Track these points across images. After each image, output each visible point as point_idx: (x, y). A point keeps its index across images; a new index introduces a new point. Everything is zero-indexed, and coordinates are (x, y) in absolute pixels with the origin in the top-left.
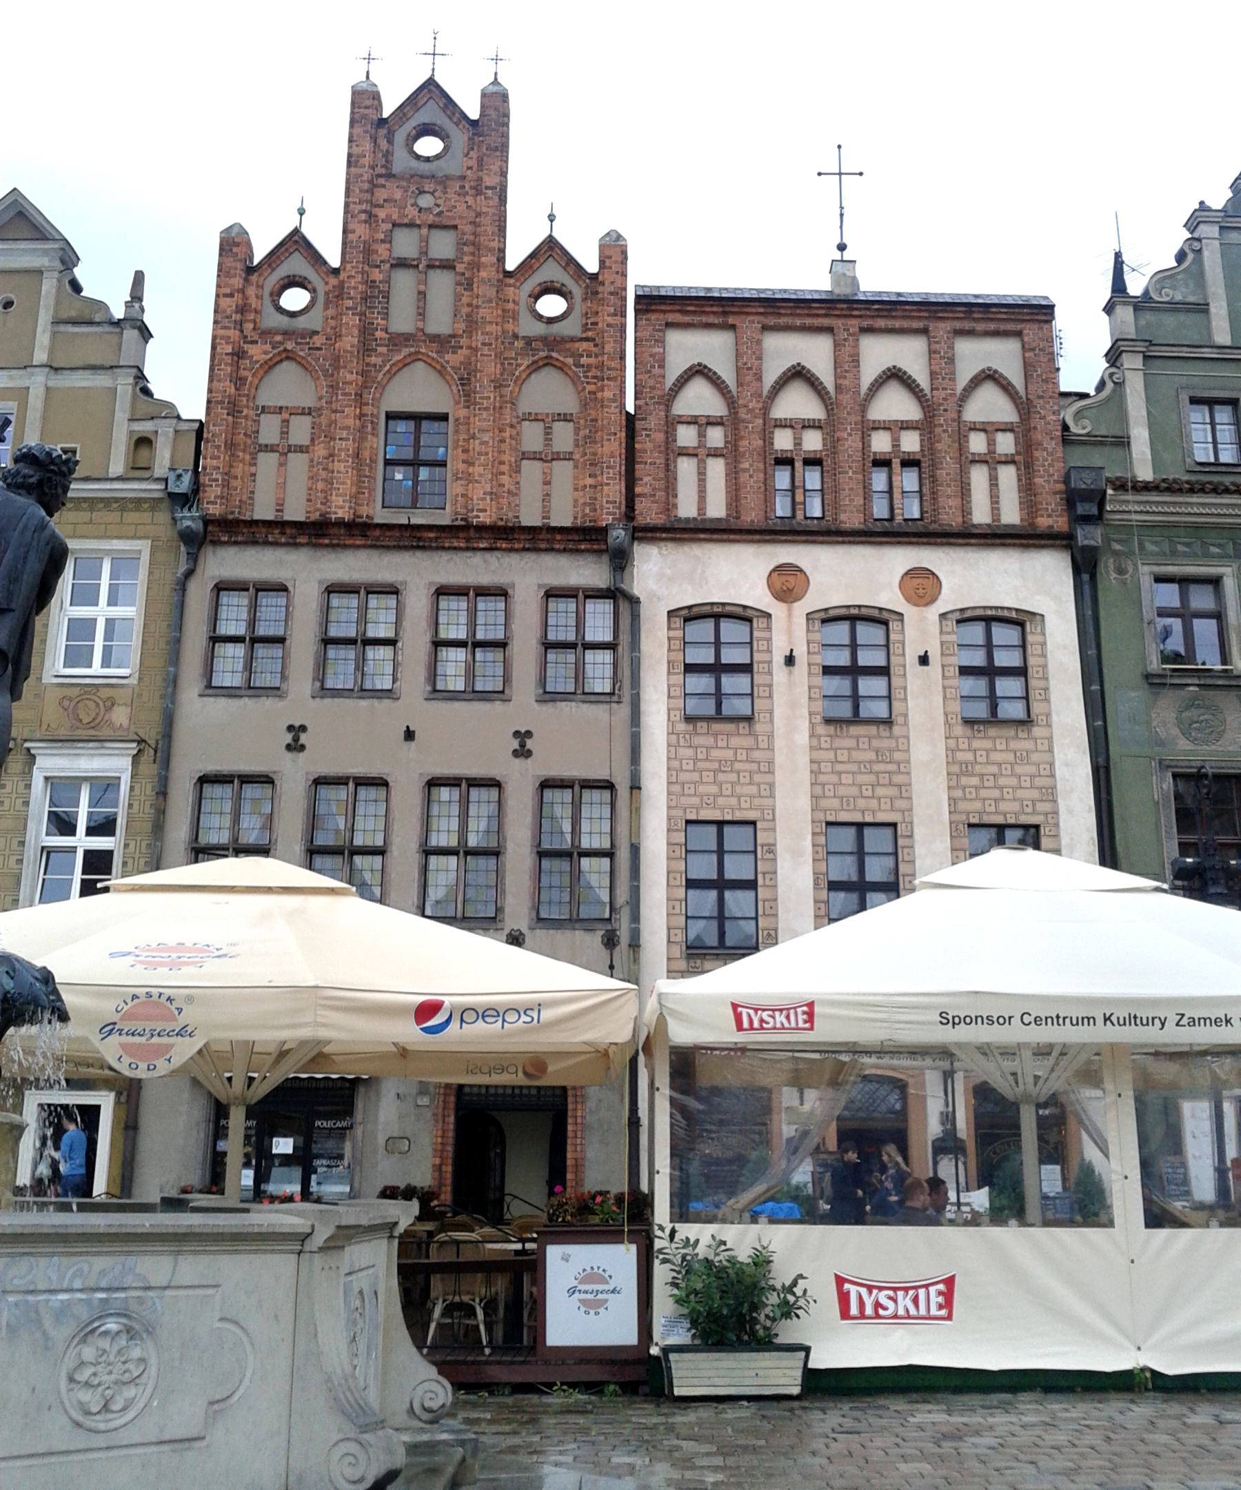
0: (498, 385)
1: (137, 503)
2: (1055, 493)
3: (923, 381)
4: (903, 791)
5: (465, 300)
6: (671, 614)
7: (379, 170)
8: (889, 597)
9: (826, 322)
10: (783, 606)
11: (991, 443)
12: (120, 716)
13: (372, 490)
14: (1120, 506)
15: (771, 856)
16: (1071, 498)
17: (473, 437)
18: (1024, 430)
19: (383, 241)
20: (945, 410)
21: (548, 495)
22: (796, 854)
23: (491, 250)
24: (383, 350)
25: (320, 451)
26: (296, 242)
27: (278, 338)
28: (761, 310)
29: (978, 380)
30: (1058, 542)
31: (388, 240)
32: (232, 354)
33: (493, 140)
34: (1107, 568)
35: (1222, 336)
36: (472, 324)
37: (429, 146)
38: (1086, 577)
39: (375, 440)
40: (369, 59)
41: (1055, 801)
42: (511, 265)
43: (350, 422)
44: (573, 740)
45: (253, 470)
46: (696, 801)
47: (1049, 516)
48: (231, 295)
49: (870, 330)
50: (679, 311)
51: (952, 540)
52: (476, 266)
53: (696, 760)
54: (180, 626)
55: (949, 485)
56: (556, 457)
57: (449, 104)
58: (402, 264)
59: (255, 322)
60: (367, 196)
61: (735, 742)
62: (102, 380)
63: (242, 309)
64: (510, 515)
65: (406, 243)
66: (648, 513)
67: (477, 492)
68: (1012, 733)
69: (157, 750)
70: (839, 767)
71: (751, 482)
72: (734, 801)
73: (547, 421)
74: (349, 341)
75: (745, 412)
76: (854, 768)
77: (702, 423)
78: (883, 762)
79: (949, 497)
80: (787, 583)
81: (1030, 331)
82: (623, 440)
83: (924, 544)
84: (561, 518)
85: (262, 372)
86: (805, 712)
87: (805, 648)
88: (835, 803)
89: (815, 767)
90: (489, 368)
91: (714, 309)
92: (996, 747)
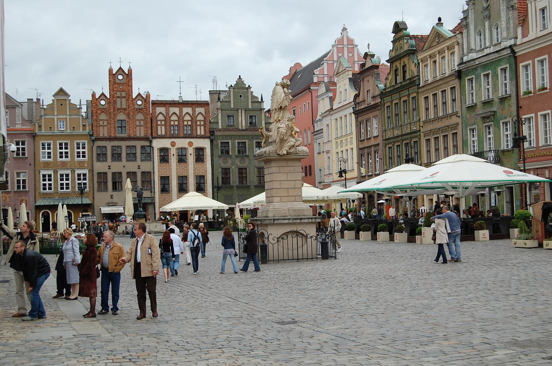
0: (133, 116)
1: (84, 135)
8: (187, 146)
12: (86, 165)
14: (217, 133)
16: (210, 132)
18: (204, 121)
29: (198, 114)
34: (215, 142)
35: (232, 107)
42: (134, 98)
44: (146, 166)
54: (92, 153)
57: (123, 71)
58: (118, 97)
62: (78, 117)
65: (118, 94)
66: (154, 135)
67: (131, 132)
69: (91, 171)
71: (168, 130)
73: (140, 120)
74: (112, 110)
75: (167, 119)
77: (161, 121)
80: (173, 144)
81: (206, 107)
84: (142, 135)
90: (132, 114)
92: (200, 165)
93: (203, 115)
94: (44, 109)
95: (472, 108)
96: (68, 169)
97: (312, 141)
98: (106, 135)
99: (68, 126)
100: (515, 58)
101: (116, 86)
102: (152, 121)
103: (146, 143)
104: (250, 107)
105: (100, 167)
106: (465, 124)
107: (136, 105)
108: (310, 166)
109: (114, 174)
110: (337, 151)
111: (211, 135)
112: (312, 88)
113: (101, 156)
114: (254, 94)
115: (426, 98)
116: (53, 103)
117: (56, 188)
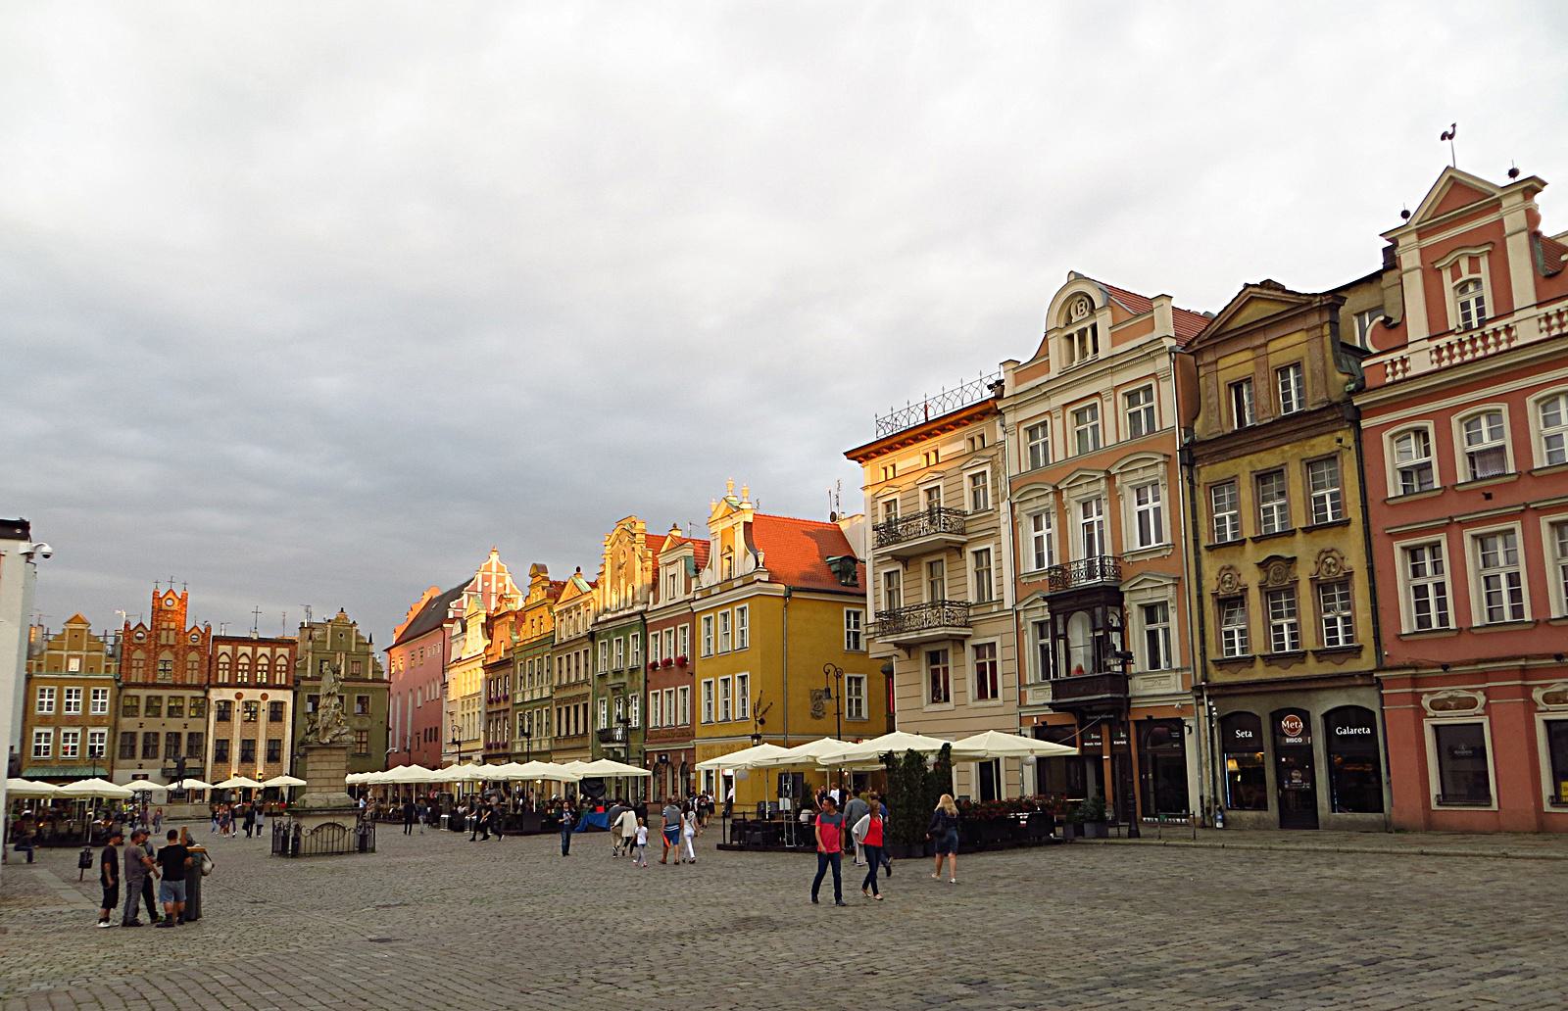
4: (257, 734)
14: (303, 683)
16: (294, 681)
18: (287, 666)
26: (141, 624)
29: (279, 657)
34: (299, 695)
35: (328, 648)
36: (178, 643)
37: (169, 602)
44: (196, 726)
57: (174, 594)
58: (164, 629)
65: (165, 625)
66: (212, 682)
69: (114, 729)
74: (152, 647)
75: (234, 661)
77: (224, 664)
80: (239, 696)
84: (195, 682)
92: (276, 725)
93: (285, 657)
94: (49, 641)
95: (603, 677)
96: (79, 726)
97: (441, 696)
98: (140, 681)
99: (84, 667)
100: (646, 625)
101: (162, 614)
102: (212, 661)
103: (199, 694)
104: (353, 650)
105: (127, 724)
106: (596, 695)
108: (436, 728)
109: (147, 734)
110: (463, 713)
111: (294, 685)
112: (445, 625)
113: (131, 711)
114: (361, 633)
115: (560, 659)
116: (63, 634)
117: (56, 751)
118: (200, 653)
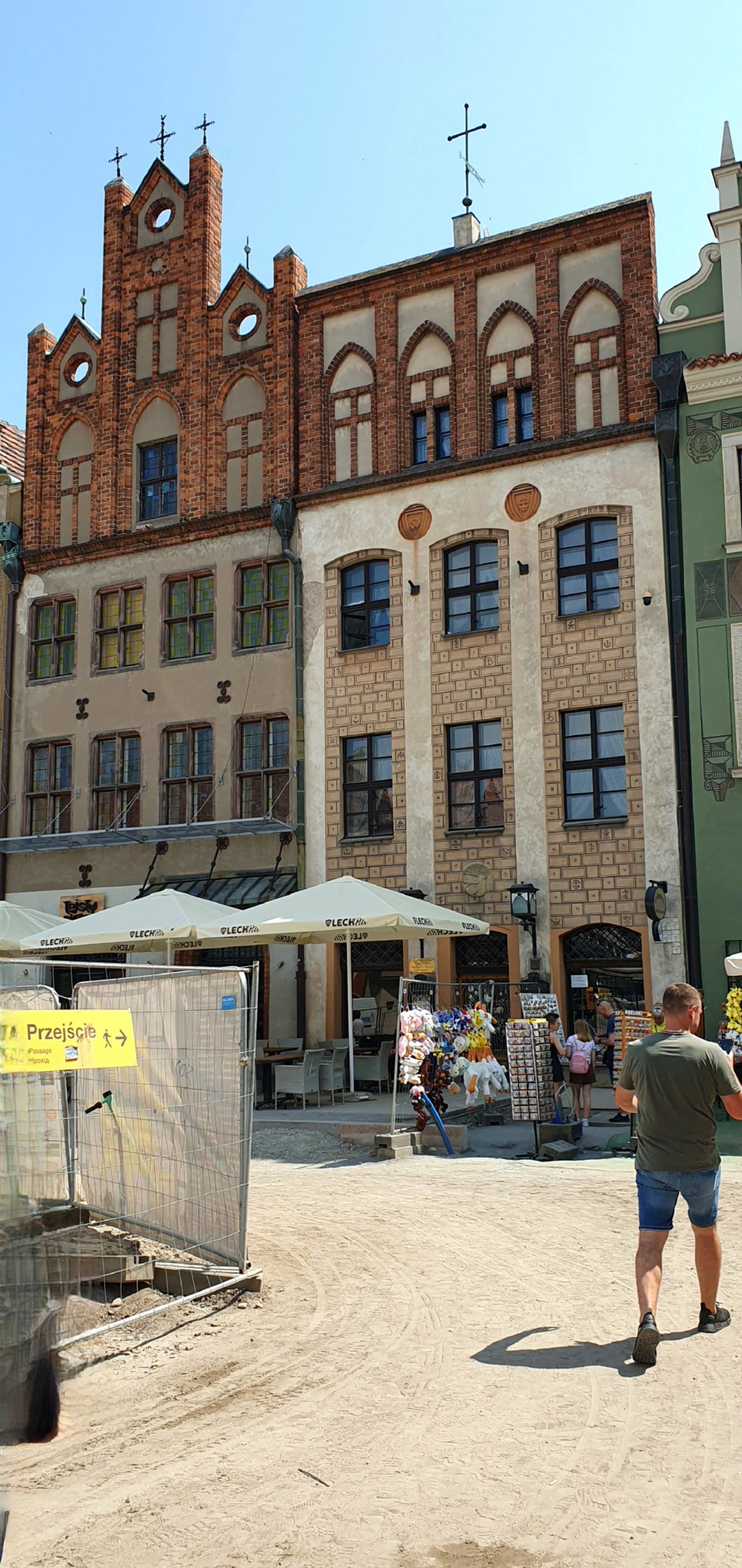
0: (205, 403)
2: (646, 386)
3: (531, 308)
5: (184, 339)
6: (327, 567)
7: (126, 251)
8: (496, 517)
9: (445, 277)
10: (411, 543)
11: (595, 351)
13: (128, 511)
15: (402, 759)
17: (188, 451)
18: (620, 332)
19: (130, 308)
20: (548, 331)
21: (245, 485)
22: (420, 755)
23: (197, 292)
24: (131, 396)
25: (95, 487)
27: (67, 406)
28: (393, 282)
30: (643, 434)
31: (135, 306)
32: (37, 427)
33: (200, 196)
38: (670, 462)
39: (129, 468)
40: (118, 158)
41: (636, 680)
43: (109, 460)
45: (58, 512)
46: (346, 720)
47: (640, 410)
48: (36, 382)
49: (485, 273)
50: (330, 302)
51: (547, 453)
52: (188, 309)
53: (346, 687)
55: (550, 402)
56: (251, 451)
58: (143, 322)
59: (54, 398)
60: (116, 275)
61: (375, 667)
63: (43, 391)
64: (218, 509)
66: (309, 483)
68: (600, 622)
70: (454, 677)
72: (374, 717)
76: (466, 675)
78: (489, 667)
79: (549, 413)
80: (413, 523)
82: (292, 426)
83: (509, 465)
85: (59, 435)
86: (428, 632)
87: (428, 577)
88: (451, 708)
89: (436, 679)
91: (356, 292)
93: (608, 292)
103: (259, 544)
107: (227, 339)
118: (268, 377)
